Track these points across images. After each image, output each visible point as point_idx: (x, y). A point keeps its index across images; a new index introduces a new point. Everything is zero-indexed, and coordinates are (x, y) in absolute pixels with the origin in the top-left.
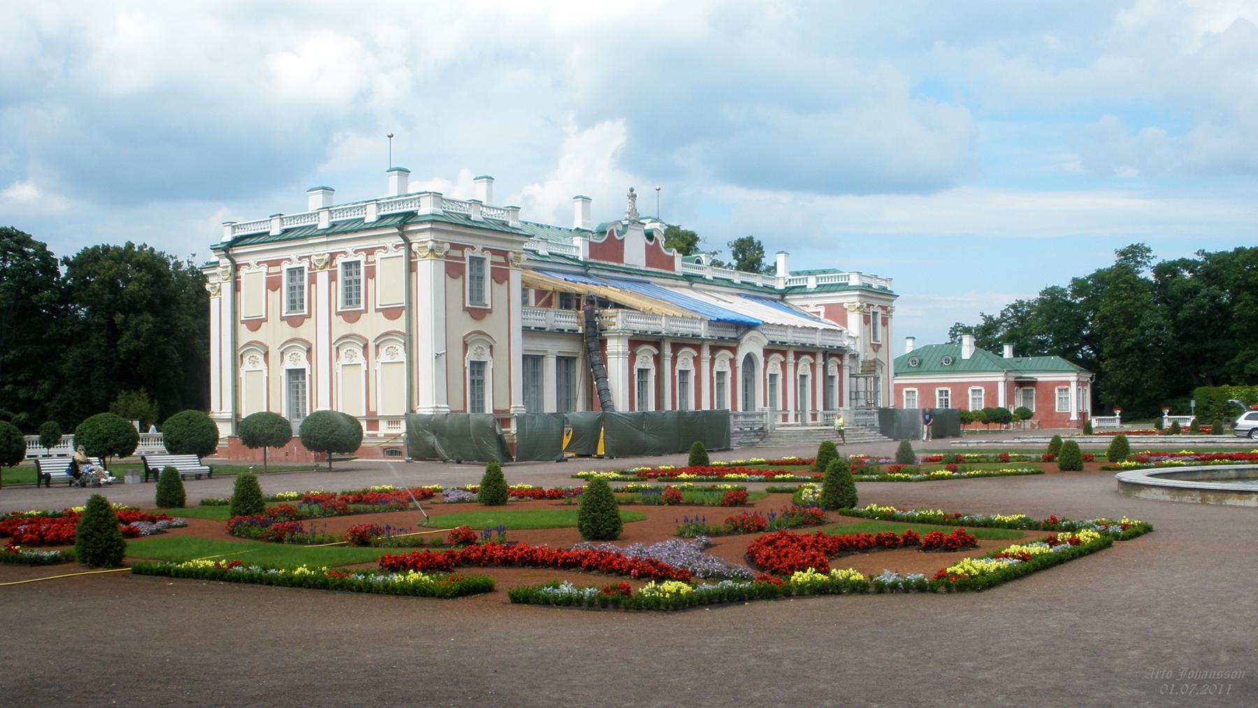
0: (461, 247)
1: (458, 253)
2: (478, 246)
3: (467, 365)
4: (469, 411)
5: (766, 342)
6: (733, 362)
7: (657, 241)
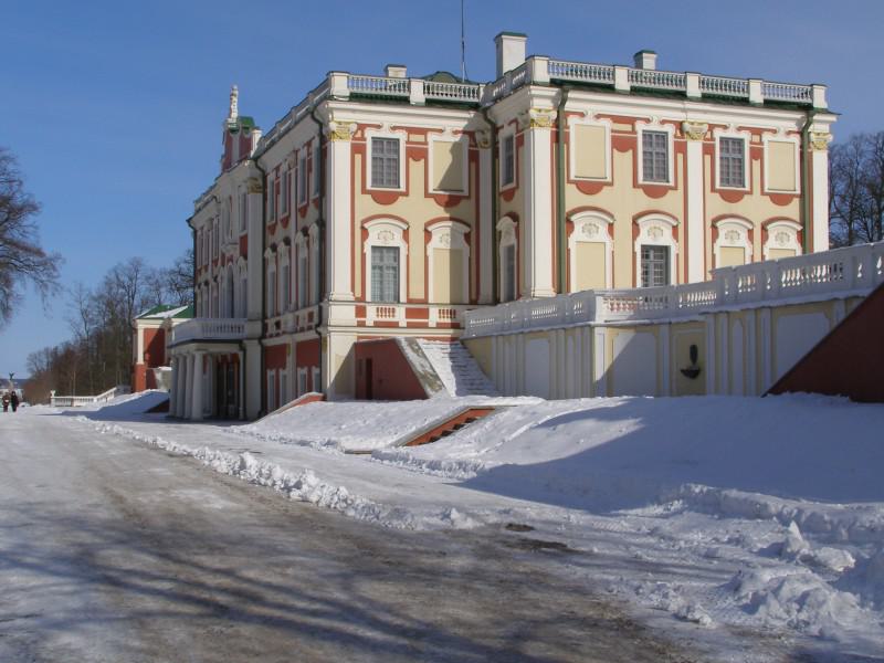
3: (368, 251)
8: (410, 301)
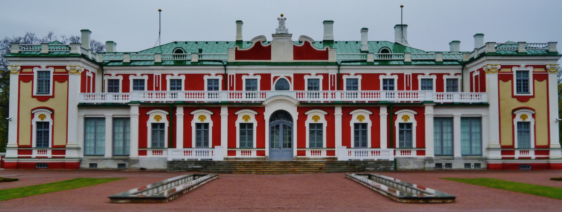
0: (32, 67)
1: (30, 70)
2: (43, 65)
4: (34, 145)
5: (296, 103)
6: (260, 118)
7: (306, 42)
8: (53, 146)
